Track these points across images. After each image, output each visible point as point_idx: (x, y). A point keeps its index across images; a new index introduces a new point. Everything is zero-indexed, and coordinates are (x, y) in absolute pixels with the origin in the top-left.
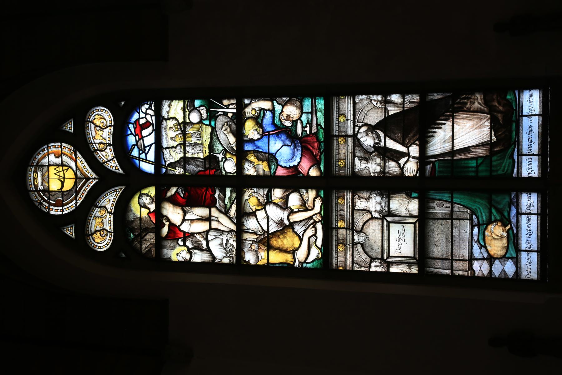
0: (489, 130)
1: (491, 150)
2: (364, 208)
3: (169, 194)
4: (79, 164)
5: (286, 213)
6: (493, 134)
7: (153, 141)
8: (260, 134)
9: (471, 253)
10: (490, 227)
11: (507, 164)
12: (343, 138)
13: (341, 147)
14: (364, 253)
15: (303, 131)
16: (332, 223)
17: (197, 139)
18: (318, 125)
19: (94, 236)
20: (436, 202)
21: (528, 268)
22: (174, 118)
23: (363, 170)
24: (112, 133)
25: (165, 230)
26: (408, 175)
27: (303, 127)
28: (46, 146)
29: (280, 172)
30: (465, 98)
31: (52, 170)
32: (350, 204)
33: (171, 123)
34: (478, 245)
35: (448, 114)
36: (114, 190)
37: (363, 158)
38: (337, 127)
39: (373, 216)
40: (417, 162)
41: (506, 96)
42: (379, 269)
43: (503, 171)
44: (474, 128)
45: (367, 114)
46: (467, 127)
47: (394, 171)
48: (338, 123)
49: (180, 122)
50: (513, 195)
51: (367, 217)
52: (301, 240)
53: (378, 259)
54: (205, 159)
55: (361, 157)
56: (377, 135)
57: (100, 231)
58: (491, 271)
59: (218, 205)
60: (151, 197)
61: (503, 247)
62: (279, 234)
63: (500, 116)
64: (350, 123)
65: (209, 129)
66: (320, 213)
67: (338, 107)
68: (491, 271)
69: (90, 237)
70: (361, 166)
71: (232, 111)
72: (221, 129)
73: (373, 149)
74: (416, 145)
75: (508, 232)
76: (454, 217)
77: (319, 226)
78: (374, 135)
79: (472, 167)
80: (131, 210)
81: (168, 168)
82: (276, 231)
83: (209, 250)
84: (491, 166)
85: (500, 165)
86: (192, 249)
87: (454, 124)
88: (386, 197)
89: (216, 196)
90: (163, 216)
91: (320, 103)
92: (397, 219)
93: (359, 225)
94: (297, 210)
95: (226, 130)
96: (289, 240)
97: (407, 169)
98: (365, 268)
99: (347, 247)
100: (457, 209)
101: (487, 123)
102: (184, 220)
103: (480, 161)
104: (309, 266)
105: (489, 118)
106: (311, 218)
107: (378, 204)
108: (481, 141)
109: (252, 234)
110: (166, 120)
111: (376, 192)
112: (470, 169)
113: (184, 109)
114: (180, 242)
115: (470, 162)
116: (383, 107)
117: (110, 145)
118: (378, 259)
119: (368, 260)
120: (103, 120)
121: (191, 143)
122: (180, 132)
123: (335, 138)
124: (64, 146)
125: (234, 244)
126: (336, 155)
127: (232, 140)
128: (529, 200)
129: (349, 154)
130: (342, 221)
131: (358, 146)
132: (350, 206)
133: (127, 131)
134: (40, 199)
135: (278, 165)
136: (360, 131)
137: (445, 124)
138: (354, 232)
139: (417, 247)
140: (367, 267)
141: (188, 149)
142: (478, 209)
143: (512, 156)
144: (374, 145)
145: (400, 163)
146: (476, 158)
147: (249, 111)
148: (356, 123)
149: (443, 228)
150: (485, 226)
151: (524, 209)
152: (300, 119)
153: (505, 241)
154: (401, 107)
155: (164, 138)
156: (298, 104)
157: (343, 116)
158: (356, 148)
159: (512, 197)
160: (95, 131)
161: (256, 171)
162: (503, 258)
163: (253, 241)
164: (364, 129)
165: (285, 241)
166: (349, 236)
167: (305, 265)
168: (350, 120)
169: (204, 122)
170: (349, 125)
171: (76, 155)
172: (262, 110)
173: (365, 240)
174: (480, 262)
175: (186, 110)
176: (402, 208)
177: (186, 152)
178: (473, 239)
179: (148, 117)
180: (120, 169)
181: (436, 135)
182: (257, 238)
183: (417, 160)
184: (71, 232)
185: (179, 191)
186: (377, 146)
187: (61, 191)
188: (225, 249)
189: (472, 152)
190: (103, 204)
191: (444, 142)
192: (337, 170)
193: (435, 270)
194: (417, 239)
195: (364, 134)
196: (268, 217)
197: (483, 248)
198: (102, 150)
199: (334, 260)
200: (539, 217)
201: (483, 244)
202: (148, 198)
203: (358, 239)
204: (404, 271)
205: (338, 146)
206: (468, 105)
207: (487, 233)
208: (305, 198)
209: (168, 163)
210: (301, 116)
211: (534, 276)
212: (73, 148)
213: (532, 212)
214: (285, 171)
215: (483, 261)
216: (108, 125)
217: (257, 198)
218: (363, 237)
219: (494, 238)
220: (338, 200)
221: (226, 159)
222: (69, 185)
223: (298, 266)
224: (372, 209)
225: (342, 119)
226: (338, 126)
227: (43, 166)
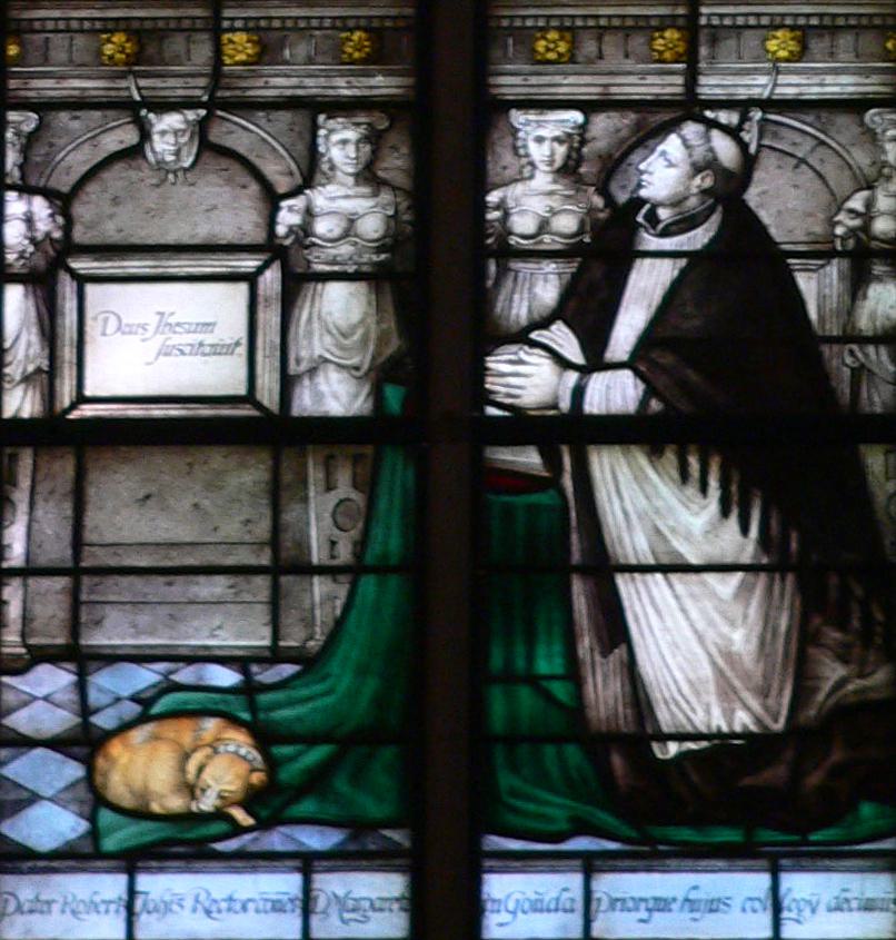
0: (709, 727)
2: (326, 159)
6: (692, 746)
9: (111, 658)
10: (239, 741)
11: (549, 811)
12: (681, 50)
13: (638, 42)
14: (95, 161)
21: (49, 903)
23: (515, 149)
26: (490, 365)
30: (867, 619)
32: (343, 88)
34: (154, 686)
35: (794, 545)
37: (578, 150)
38: (740, 21)
39: (284, 204)
40: (555, 406)
41: (872, 797)
42: (14, 233)
43: (514, 793)
44: (720, 662)
45: (804, 167)
46: (725, 629)
47: (511, 300)
48: (759, 27)
50: (396, 835)
55: (583, 142)
56: (693, 217)
58: (25, 743)
61: (144, 795)
63: (776, 774)
64: (758, 85)
67: (841, 22)
68: (25, 743)
70: (540, 140)
73: (622, 197)
74: (644, 403)
75: (219, 815)
76: (284, 580)
78: (693, 202)
79: (530, 658)
84: (537, 740)
85: (542, 779)
87: (739, 576)
92: (270, 318)
93: (239, 134)
97: (521, 362)
98: (21, 167)
99: (123, 76)
101: (742, 720)
103: (560, 690)
105: (766, 728)
107: (344, 224)
108: (656, 696)
111: (406, 217)
112: (520, 649)
115: (558, 648)
116: (832, 242)
119: (64, 183)
123: (681, 11)
126: (597, 17)
128: (372, 906)
130: (257, 49)
131: (638, 126)
132: (331, 92)
136: (715, 134)
137: (745, 530)
138: (203, 112)
139: (134, 411)
140: (23, 178)
143: (582, 828)
145: (554, 327)
146: (574, 674)
148: (757, 115)
149: (231, 529)
150: (246, 716)
151: (331, 884)
153: (176, 803)
154: (834, 329)
157: (793, 46)
158: (630, 118)
159: (387, 833)
164: (725, 148)
166: (174, 88)
168: (775, 85)
170: (747, 80)
173: (160, 166)
174: (71, 697)
176: (328, 339)
178: (181, 665)
181: (692, 490)
183: (565, 405)
186: (640, 219)
189: (605, 653)
191: (658, 531)
192: (518, 23)
193: (21, 497)
194: (174, 411)
199: (57, 14)
201: (156, 709)
203: (163, 133)
204: (13, 351)
205: (641, 28)
206: (834, 635)
207: (211, 725)
213: (315, 921)
215: (76, 707)
218: (177, 153)
219: (186, 756)
220: (365, 30)
224: (320, 198)
225: (780, 43)
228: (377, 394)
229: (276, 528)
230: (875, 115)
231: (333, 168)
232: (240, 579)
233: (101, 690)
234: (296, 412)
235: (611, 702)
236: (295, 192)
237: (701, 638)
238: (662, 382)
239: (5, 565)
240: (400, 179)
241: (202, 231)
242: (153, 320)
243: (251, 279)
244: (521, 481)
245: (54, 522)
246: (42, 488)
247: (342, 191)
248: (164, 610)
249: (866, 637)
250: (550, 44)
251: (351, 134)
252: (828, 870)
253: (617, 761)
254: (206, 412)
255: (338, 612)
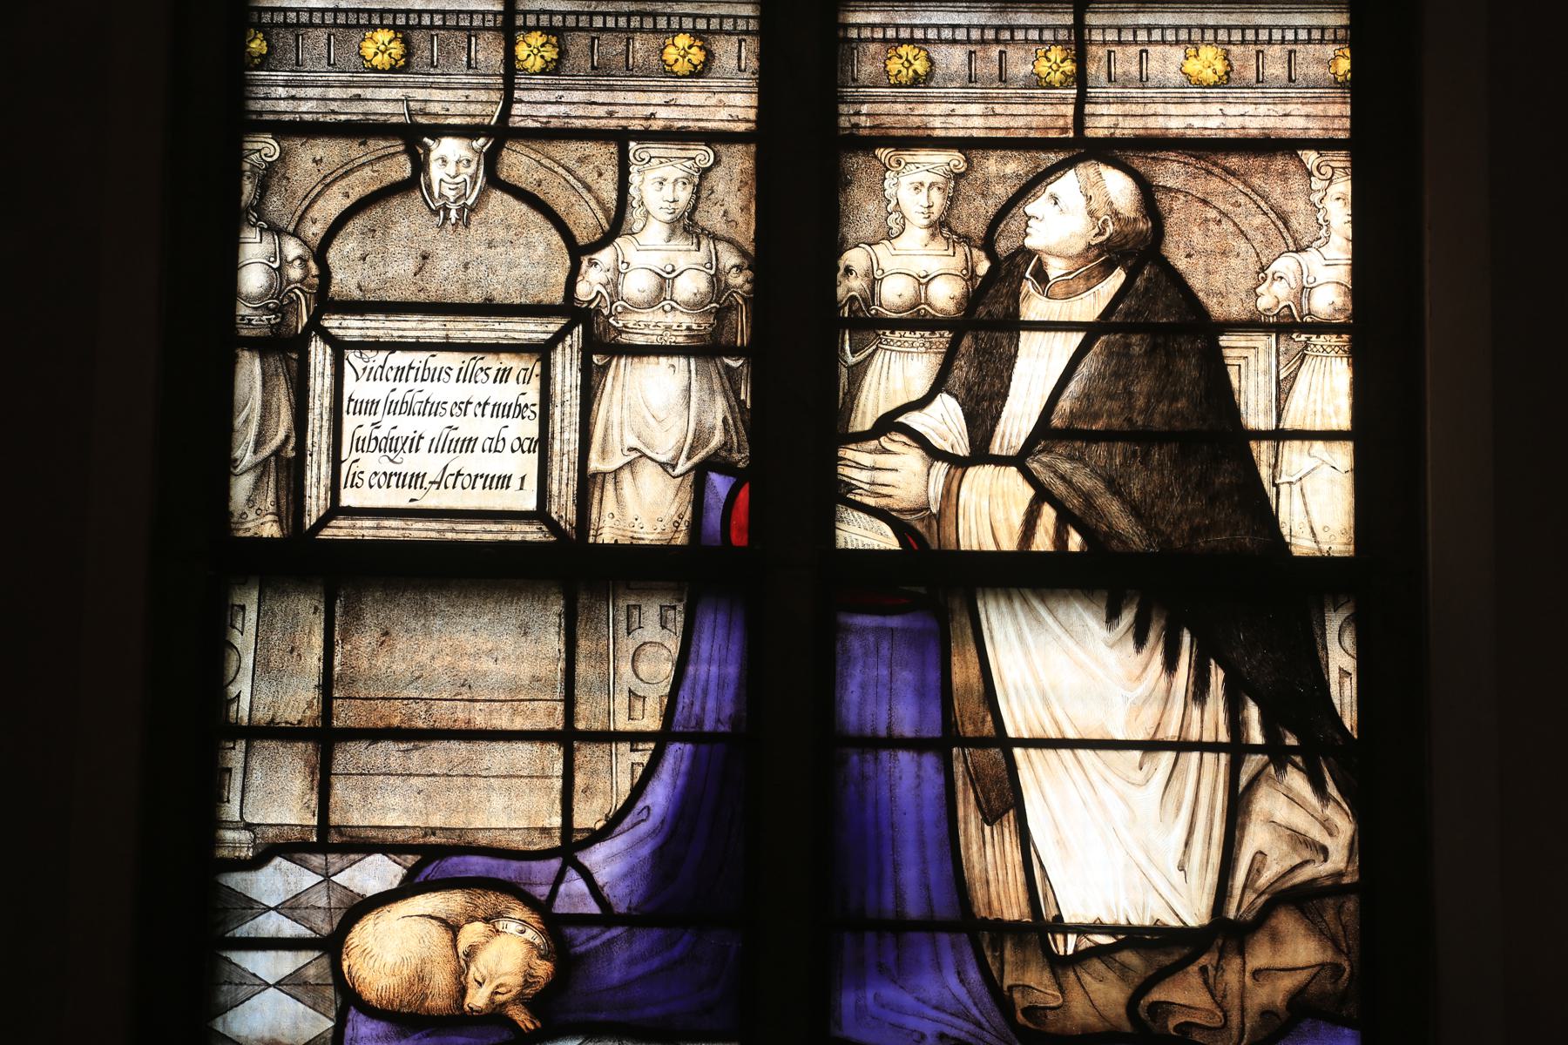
42: (253, 279)
97: (885, 451)
144: (1029, 254)
251: (674, 172)
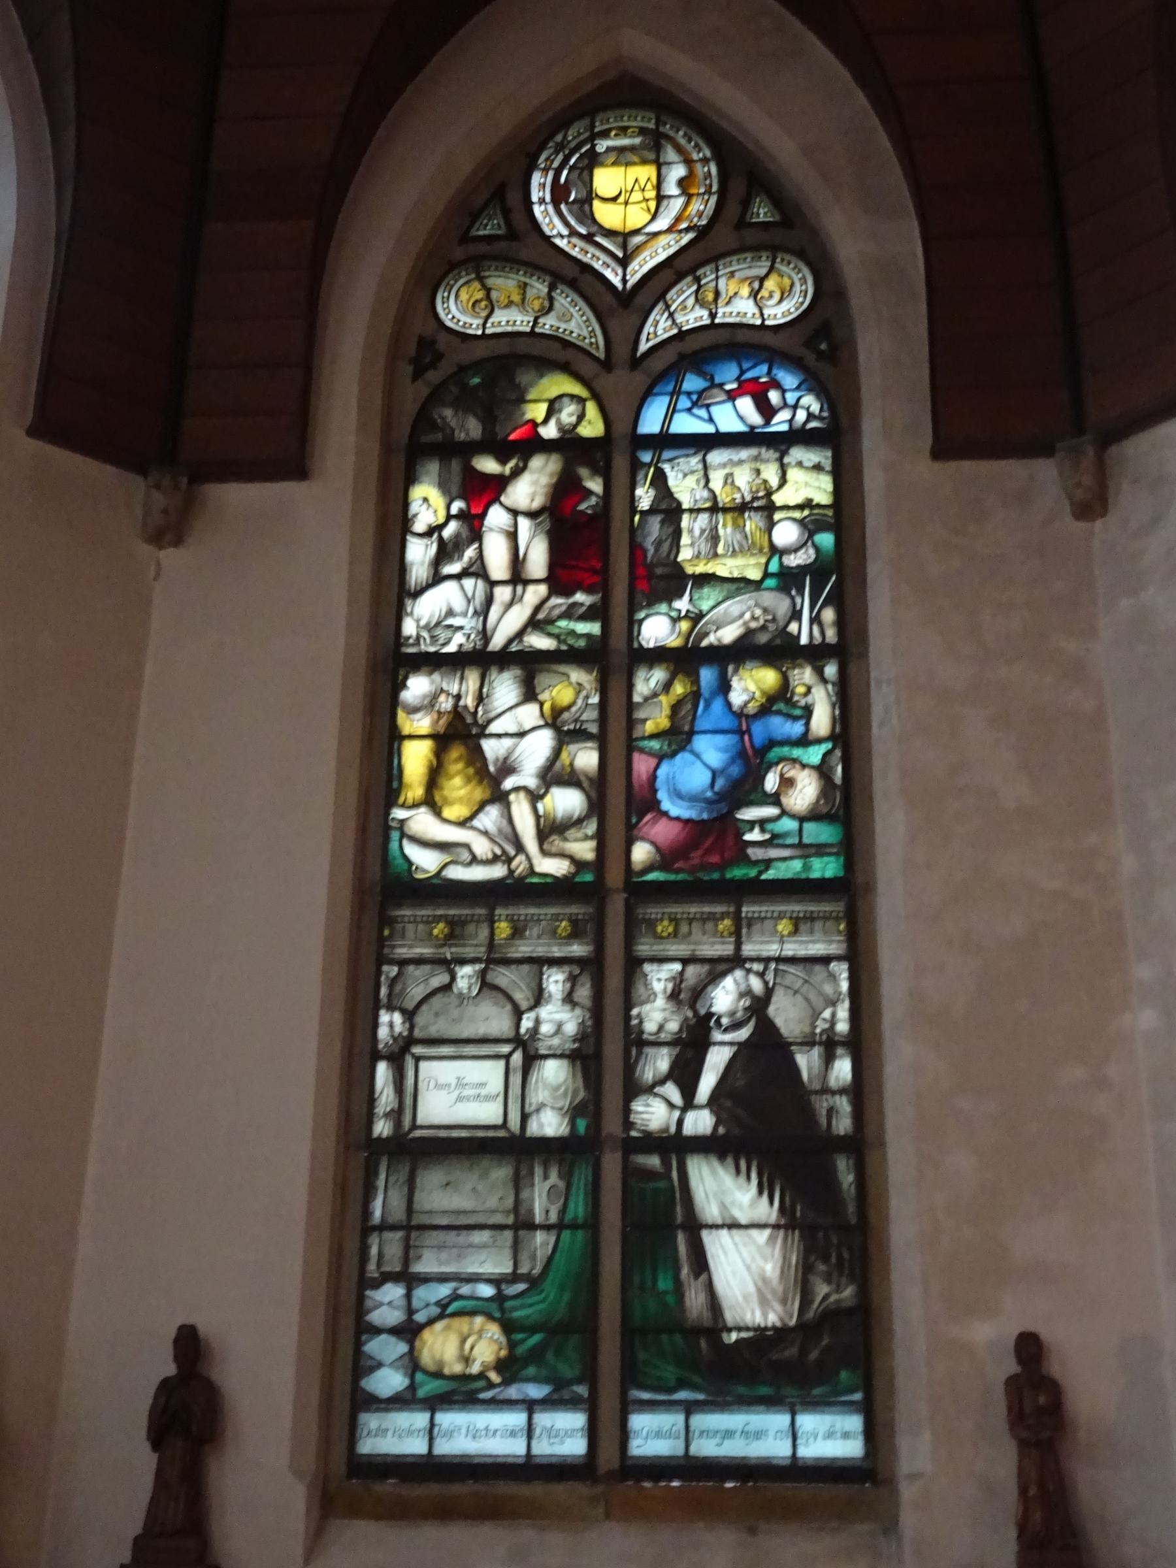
1: (698, 1331)
3: (583, 472)
4: (663, 240)
5: (532, 782)
6: (744, 1335)
7: (723, 429)
8: (742, 711)
9: (425, 1279)
10: (494, 1330)
13: (709, 925)
15: (752, 824)
16: (506, 905)
17: (730, 542)
18: (768, 863)
19: (476, 285)
20: (562, 1185)
22: (783, 481)
23: (646, 985)
24: (745, 321)
25: (488, 465)
27: (762, 823)
28: (708, 154)
29: (642, 765)
30: (840, 1257)
31: (646, 173)
32: (557, 952)
33: (771, 474)
34: (448, 1296)
36: (593, 330)
40: (667, 1130)
42: (383, 1033)
46: (761, 1262)
49: (775, 497)
51: (522, 997)
52: (463, 823)
53: (412, 1028)
54: (678, 567)
55: (681, 982)
57: (488, 297)
58: (377, 1331)
59: (556, 601)
60: (575, 426)
61: (441, 1363)
62: (478, 765)
63: (791, 1352)
64: (773, 949)
65: (754, 574)
66: (532, 872)
68: (377, 1331)
69: (473, 276)
70: (659, 980)
71: (804, 632)
72: (755, 606)
73: (702, 1012)
75: (481, 1376)
76: (522, 1233)
77: (497, 872)
80: (542, 376)
81: (652, 470)
82: (484, 759)
83: (437, 579)
86: (441, 539)
88: (574, 1050)
89: (579, 597)
90: (526, 460)
91: (826, 868)
92: (516, 1080)
93: (503, 977)
94: (541, 812)
95: (754, 618)
96: (462, 792)
97: (648, 1105)
99: (442, 946)
100: (541, 1242)
101: (773, 1319)
102: (515, 513)
103: (670, 1299)
104: (394, 845)
106: (520, 848)
109: (477, 693)
110: (780, 460)
113: (808, 504)
114: (457, 506)
117: (713, 316)
118: (412, 1028)
119: (410, 1005)
120: (777, 296)
121: (720, 526)
122: (748, 498)
124: (708, 200)
125: (451, 648)
127: (728, 634)
129: (692, 947)
131: (710, 973)
133: (747, 359)
134: (572, 145)
135: (661, 757)
137: (771, 1202)
139: (443, 1134)
141: (703, 519)
142: (543, 1295)
143: (682, 1384)
146: (679, 1290)
147: (803, 676)
149: (492, 1202)
150: (497, 1315)
151: (544, 1419)
152: (784, 813)
153: (458, 1368)
154: (816, 1086)
155: (731, 457)
156: (825, 810)
157: (790, 928)
158: (706, 967)
160: (747, 279)
161: (646, 699)
162: (412, 1364)
163: (458, 697)
165: (457, 781)
166: (469, 952)
167: (395, 835)
169: (775, 560)
171: (687, 230)
172: (808, 711)
173: (461, 994)
174: (403, 1302)
175: (806, 512)
177: (694, 515)
179: (784, 415)
180: (651, 344)
181: (742, 1179)
182: (466, 707)
183: (673, 1129)
184: (490, 227)
185: (593, 500)
187: (589, 196)
188: (438, 624)
190: (556, 305)
194: (464, 1134)
195: (743, 987)
196: (521, 734)
197: (438, 1310)
198: (699, 297)
200: (521, 1461)
201: (450, 1310)
202: (574, 419)
203: (462, 977)
206: (822, 1267)
207: (479, 1320)
208: (572, 833)
209: (666, 467)
210: (793, 816)
211: (367, 1446)
212: (704, 222)
213: (534, 1443)
214: (644, 777)
216: (766, 312)
217: (573, 703)
218: (470, 988)
219: (463, 1341)
221: (675, 620)
222: (608, 215)
223: (393, 819)
224: (545, 1012)
225: (784, 926)
226: (765, 918)
227: (657, 148)
228: (573, 1124)
229: (517, 1202)
230: (834, 966)
231: (550, 996)
232: (498, 1232)
233: (419, 1299)
234: (529, 1134)
235: (699, 1307)
236: (531, 1009)
237: (748, 1268)
238: (724, 1116)
239: (370, 1224)
240: (588, 1003)
241: (481, 1030)
242: (454, 1082)
243: (507, 1057)
244: (649, 1174)
245: (397, 1200)
246: (392, 1179)
247: (555, 1009)
248: (455, 1251)
249: (840, 1265)
250: (665, 927)
252: (823, 1412)
253: (703, 1343)
254: (481, 1134)
255: (550, 1252)
